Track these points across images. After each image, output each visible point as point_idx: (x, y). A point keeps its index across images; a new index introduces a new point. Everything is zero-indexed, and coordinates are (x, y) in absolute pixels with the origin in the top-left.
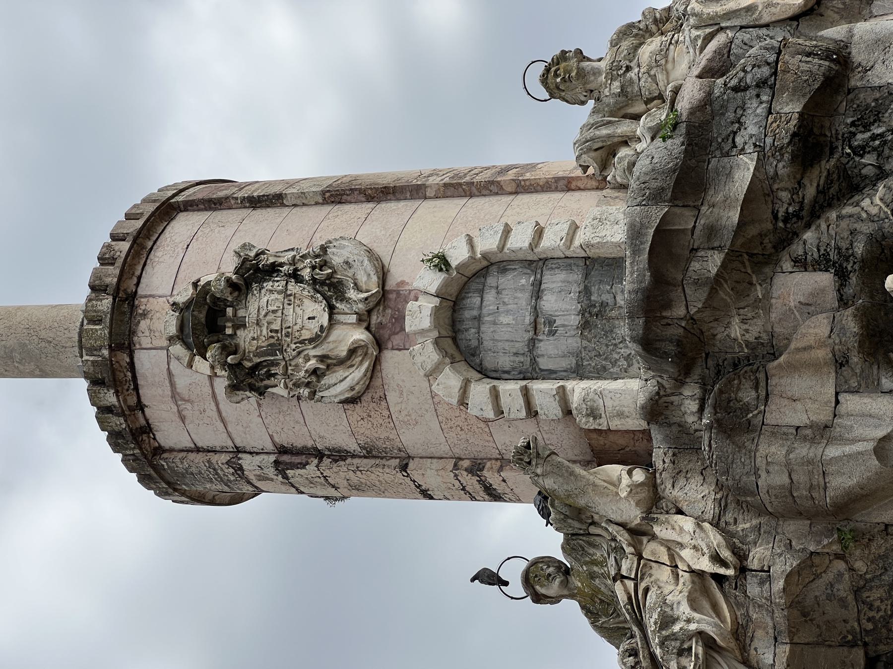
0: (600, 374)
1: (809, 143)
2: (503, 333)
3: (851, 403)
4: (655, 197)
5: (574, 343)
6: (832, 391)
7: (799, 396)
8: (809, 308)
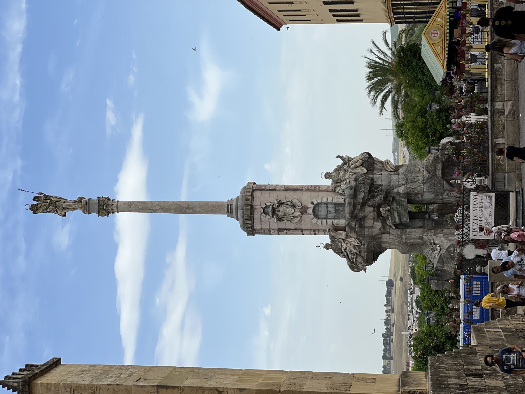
0: (337, 219)
1: (370, 191)
2: (322, 213)
3: (375, 223)
4: (352, 198)
5: (334, 215)
7: (369, 223)
8: (370, 212)
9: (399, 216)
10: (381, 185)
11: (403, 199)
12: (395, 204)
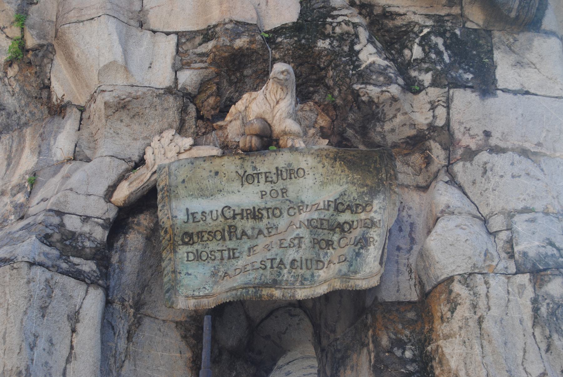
6: (180, 29)
9: (231, 228)
10: (486, 85)
11: (373, 254)
12: (331, 192)
